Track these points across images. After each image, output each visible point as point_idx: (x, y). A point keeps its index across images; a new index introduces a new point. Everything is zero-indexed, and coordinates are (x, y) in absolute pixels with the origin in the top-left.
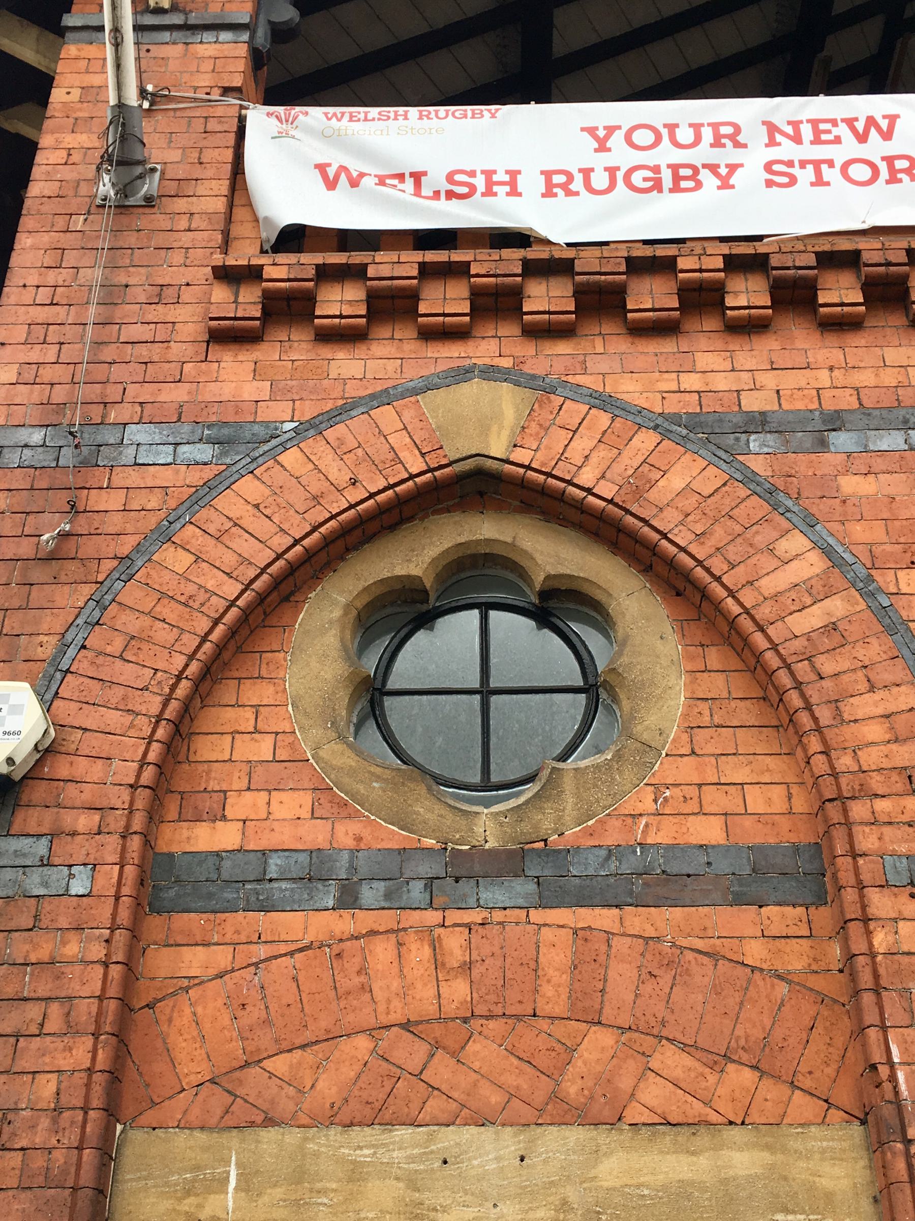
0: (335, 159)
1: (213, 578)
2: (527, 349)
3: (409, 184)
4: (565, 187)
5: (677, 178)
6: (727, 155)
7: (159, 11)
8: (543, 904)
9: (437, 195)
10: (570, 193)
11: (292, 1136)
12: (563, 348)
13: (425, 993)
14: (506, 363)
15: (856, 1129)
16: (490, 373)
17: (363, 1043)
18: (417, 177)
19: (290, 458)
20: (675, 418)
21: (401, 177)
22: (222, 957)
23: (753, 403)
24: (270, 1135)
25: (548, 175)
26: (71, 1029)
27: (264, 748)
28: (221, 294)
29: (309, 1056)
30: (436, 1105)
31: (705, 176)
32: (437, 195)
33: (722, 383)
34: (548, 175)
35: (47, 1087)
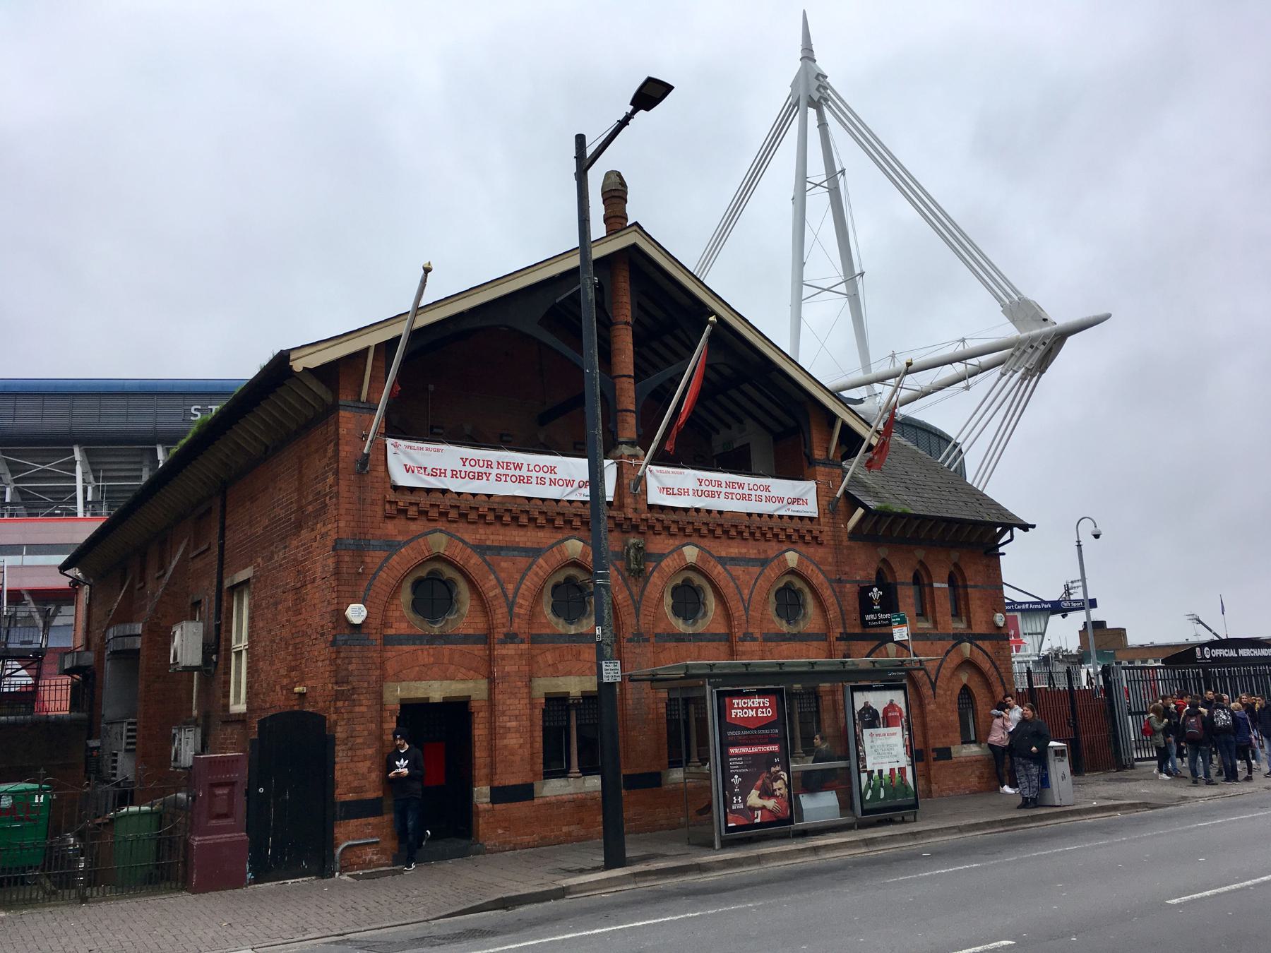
0: (409, 463)
1: (391, 581)
2: (448, 525)
3: (423, 471)
4: (455, 475)
5: (478, 476)
6: (488, 471)
7: (363, 402)
8: (445, 645)
9: (429, 475)
10: (457, 477)
11: (407, 683)
12: (455, 525)
13: (426, 660)
14: (443, 528)
15: (487, 680)
16: (441, 531)
17: (417, 668)
18: (425, 468)
19: (403, 550)
20: (473, 545)
21: (421, 468)
22: (394, 653)
23: (488, 543)
24: (403, 683)
25: (452, 471)
26: (377, 668)
27: (397, 614)
28: (387, 506)
29: (409, 670)
30: (428, 678)
31: (484, 475)
32: (429, 475)
33: (483, 537)
34: (452, 471)
35: (374, 678)
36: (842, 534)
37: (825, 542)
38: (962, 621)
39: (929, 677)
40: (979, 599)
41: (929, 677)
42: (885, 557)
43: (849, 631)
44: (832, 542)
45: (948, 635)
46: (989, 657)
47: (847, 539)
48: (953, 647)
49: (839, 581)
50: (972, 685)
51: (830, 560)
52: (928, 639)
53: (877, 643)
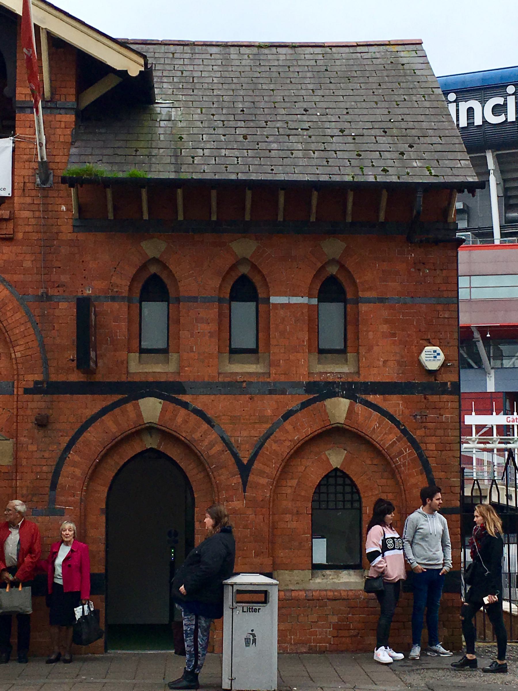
36: (60, 222)
37: (20, 236)
38: (346, 360)
39: (235, 455)
40: (386, 321)
41: (235, 455)
42: (158, 256)
43: (54, 378)
44: (35, 236)
45: (296, 385)
46: (397, 423)
47: (71, 230)
48: (305, 405)
49: (46, 298)
50: (352, 471)
51: (27, 264)
52: (243, 392)
53: (117, 397)
